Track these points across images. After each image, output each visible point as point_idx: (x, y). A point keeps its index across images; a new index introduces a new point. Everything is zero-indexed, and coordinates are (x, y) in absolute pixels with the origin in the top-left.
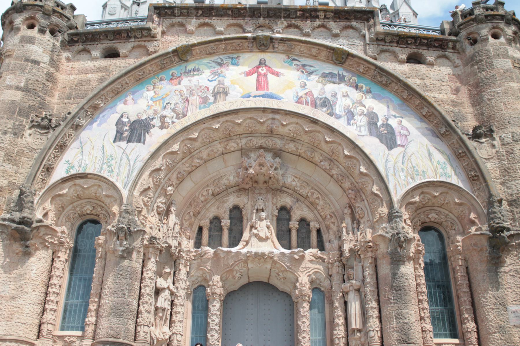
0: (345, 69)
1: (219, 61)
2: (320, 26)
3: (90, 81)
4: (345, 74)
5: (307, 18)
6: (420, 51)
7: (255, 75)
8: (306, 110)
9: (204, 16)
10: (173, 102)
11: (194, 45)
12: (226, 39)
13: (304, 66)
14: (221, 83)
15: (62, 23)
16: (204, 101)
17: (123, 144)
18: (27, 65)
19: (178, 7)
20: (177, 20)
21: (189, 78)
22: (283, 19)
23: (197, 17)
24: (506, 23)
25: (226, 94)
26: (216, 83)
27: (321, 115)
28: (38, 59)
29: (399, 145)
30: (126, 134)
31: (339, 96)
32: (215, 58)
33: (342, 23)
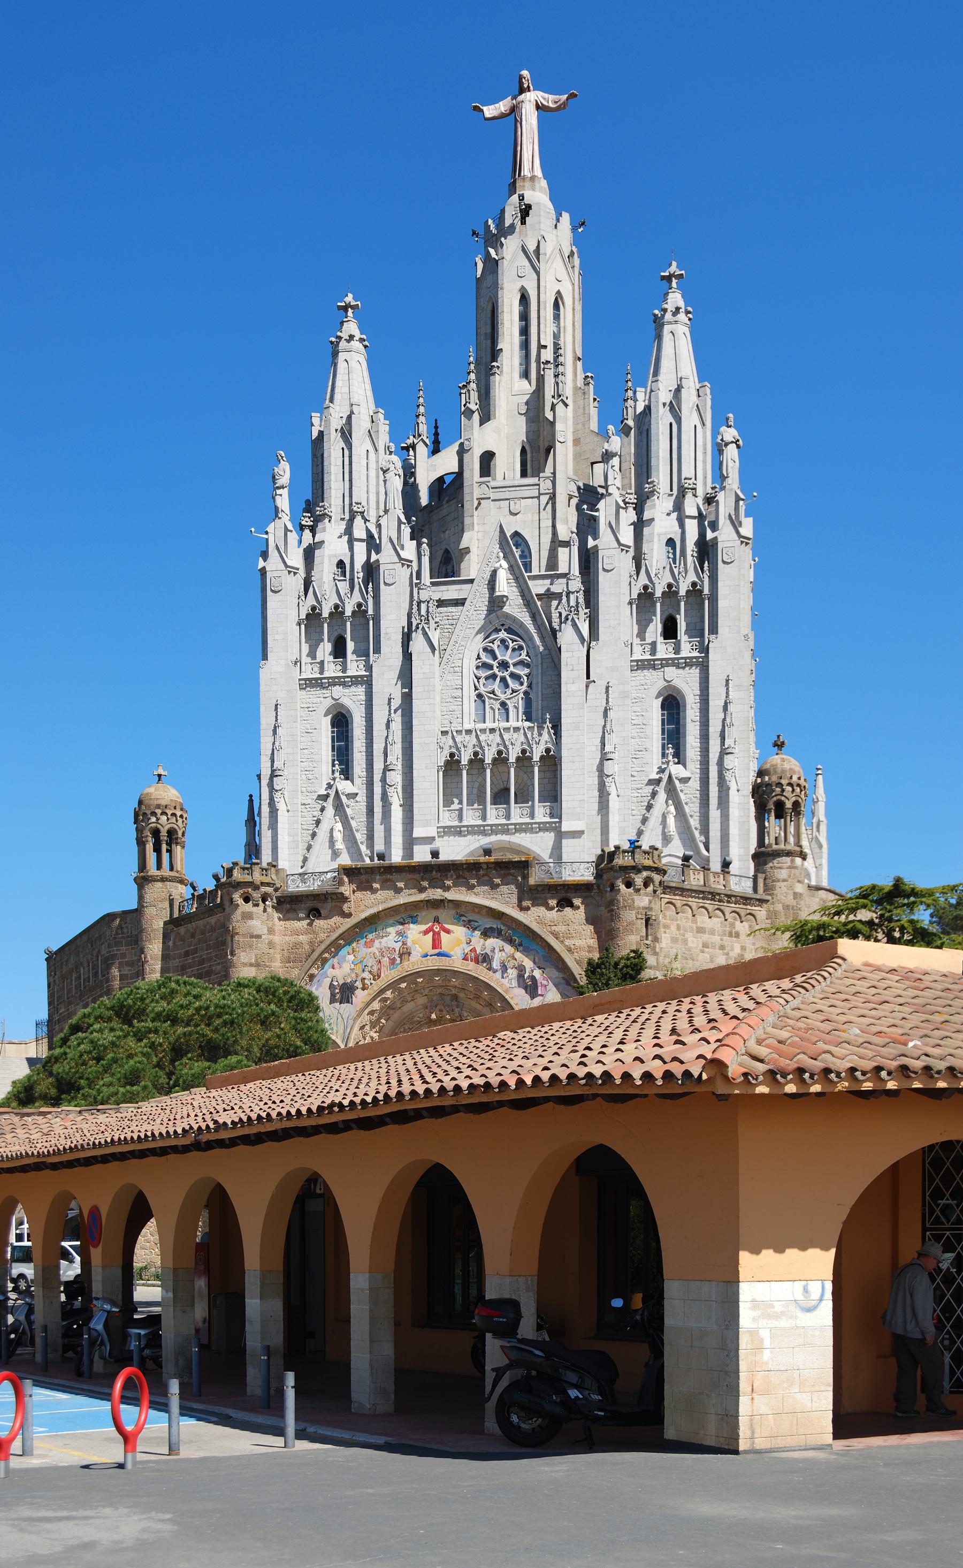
0: (502, 923)
1: (402, 920)
2: (483, 875)
4: (503, 928)
6: (569, 894)
7: (431, 934)
8: (471, 968)
10: (370, 965)
11: (380, 912)
13: (470, 921)
14: (404, 944)
16: (393, 961)
17: (337, 1005)
20: (364, 877)
21: (379, 940)
23: (381, 874)
25: (409, 954)
26: (400, 944)
27: (481, 972)
28: (259, 932)
29: (540, 995)
30: (338, 996)
31: (497, 951)
32: (397, 918)
33: (502, 872)
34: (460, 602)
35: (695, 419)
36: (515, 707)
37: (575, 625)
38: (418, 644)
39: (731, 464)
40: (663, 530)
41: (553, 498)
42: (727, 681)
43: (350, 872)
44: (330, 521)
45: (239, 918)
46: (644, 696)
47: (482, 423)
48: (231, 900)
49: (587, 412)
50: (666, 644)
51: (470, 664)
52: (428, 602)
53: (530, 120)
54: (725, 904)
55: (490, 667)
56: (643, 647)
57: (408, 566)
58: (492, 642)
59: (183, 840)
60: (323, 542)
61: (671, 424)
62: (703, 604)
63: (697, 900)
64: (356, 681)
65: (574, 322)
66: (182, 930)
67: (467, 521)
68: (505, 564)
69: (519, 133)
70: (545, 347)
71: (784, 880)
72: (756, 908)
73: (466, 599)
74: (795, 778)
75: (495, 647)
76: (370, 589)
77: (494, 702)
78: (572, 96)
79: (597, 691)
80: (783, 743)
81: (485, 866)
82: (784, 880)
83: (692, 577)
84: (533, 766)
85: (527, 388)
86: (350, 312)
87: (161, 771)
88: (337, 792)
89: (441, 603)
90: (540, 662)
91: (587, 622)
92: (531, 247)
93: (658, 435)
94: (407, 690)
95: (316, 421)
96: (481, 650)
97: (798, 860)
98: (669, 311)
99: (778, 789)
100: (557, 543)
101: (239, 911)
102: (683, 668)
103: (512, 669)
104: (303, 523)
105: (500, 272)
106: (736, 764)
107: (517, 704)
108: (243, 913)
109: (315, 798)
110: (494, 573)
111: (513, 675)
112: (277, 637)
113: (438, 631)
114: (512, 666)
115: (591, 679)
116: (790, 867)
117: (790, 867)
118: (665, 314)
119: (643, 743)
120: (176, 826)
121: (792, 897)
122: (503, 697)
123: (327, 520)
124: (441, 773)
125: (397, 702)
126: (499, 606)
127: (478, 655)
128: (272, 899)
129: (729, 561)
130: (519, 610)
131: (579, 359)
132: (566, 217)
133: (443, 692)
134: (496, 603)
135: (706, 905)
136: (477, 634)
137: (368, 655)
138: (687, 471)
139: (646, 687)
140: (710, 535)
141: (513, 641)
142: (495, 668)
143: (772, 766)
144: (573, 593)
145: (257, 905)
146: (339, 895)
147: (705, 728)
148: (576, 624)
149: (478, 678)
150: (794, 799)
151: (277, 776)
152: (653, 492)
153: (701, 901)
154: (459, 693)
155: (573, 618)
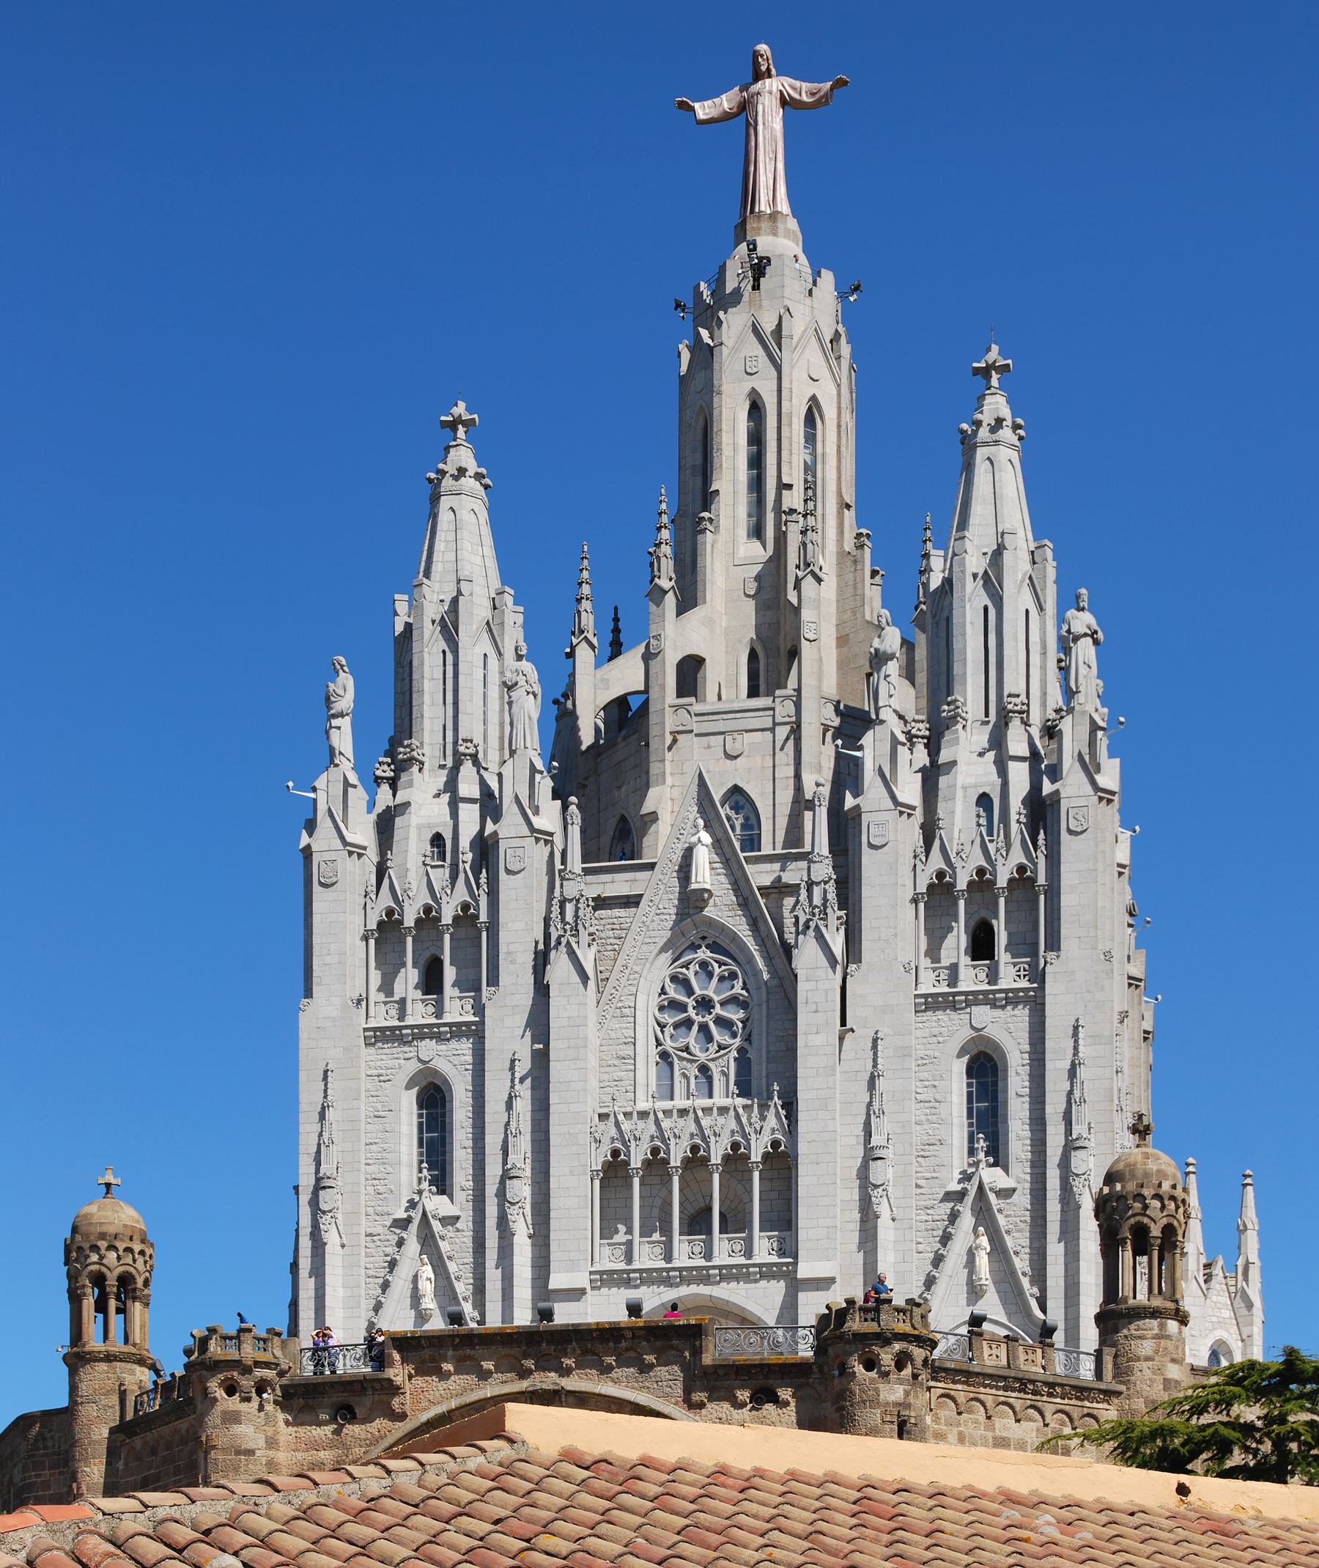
2: (627, 1350)
3: (324, 1464)
5: (608, 1339)
9: (464, 1345)
12: (492, 1398)
15: (269, 1374)
18: (240, 1460)
19: (424, 1337)
20: (427, 1353)
22: (574, 1343)
23: (455, 1348)
24: (883, 1342)
28: (251, 1445)
34: (631, 901)
35: (1027, 600)
36: (723, 1073)
37: (820, 938)
38: (559, 969)
39: (1083, 670)
40: (972, 781)
41: (796, 731)
42: (1076, 1028)
43: (406, 1344)
44: (420, 770)
45: (218, 1421)
46: (937, 1054)
47: (681, 610)
48: (205, 1391)
49: (859, 592)
50: (975, 967)
51: (647, 1004)
52: (578, 901)
53: (771, 121)
54: (1045, 1398)
55: (682, 1007)
56: (936, 973)
57: (546, 842)
58: (686, 966)
59: (146, 1292)
60: (407, 804)
61: (986, 609)
62: (1037, 901)
63: (994, 1391)
64: (458, 1031)
65: (839, 447)
66: (138, 1442)
67: (654, 769)
68: (706, 838)
69: (753, 144)
70: (789, 487)
71: (1147, 1359)
72: (1100, 1406)
73: (641, 895)
74: (1166, 1186)
75: (690, 975)
76: (483, 881)
77: (689, 1065)
78: (840, 84)
79: (857, 1045)
80: (1147, 1128)
81: (629, 1335)
82: (1147, 1359)
83: (1017, 857)
84: (750, 1171)
85: (758, 553)
86: (461, 431)
87: (110, 1178)
88: (424, 1214)
89: (601, 903)
90: (764, 999)
91: (842, 931)
92: (768, 326)
93: (964, 626)
94: (541, 1046)
95: (402, 607)
96: (668, 980)
97: (1172, 1326)
98: (985, 424)
99: (1138, 1205)
100: (803, 804)
101: (219, 1408)
102: (1003, 1007)
103: (718, 1010)
104: (379, 773)
105: (716, 366)
106: (1091, 1166)
107: (725, 1068)
108: (224, 1412)
109: (388, 1224)
110: (688, 854)
111: (720, 1021)
112: (328, 959)
113: (594, 948)
114: (718, 1006)
115: (848, 1026)
116: (1157, 1337)
117: (1157, 1337)
118: (978, 429)
119: (937, 1132)
120: (132, 1270)
121: (1161, 1387)
122: (702, 1057)
123: (415, 769)
124: (597, 1183)
125: (524, 1066)
126: (697, 907)
127: (663, 988)
128: (274, 1390)
129: (1079, 829)
130: (730, 914)
131: (848, 507)
132: (827, 278)
133: (604, 1048)
134: (691, 902)
135: (1011, 1400)
136: (660, 952)
137: (478, 989)
138: (1013, 682)
139: (941, 1039)
140: (1047, 787)
141: (721, 964)
142: (690, 1009)
143: (1128, 1165)
144: (818, 884)
145: (248, 1400)
146: (385, 1383)
147: (1039, 1106)
148: (822, 936)
149: (662, 1026)
150: (1165, 1221)
151: (324, 1188)
152: (954, 717)
153: (1001, 1393)
154: (629, 1051)
155: (817, 926)
